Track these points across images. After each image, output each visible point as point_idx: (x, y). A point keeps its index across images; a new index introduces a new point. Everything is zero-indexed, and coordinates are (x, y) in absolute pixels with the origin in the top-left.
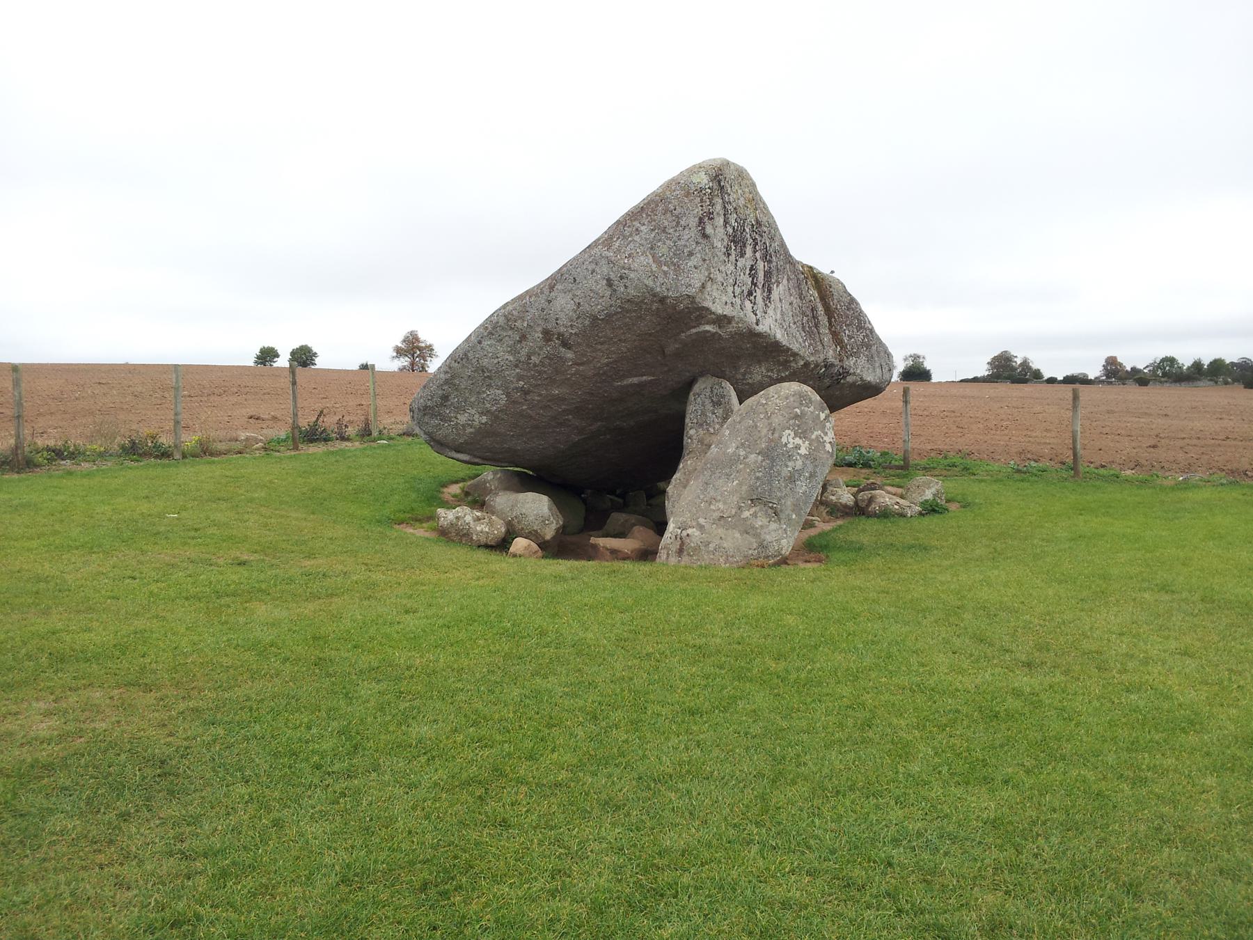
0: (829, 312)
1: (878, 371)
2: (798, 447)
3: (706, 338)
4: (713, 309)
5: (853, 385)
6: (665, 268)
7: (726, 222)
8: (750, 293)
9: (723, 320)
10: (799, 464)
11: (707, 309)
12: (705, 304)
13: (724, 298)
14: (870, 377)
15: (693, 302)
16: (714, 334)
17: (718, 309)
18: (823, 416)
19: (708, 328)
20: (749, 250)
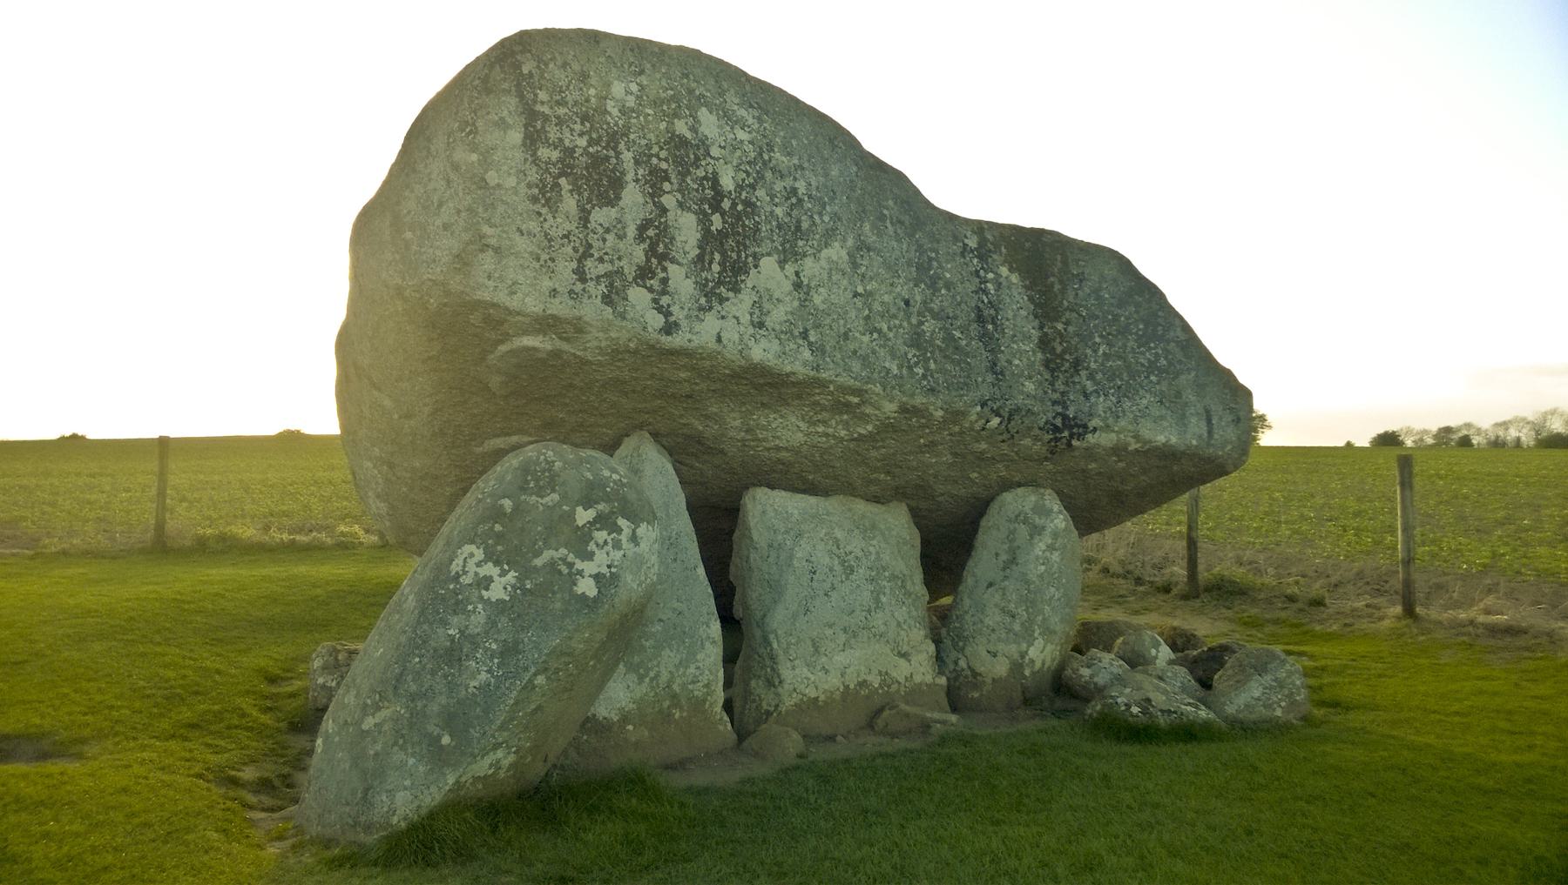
0: (1046, 310)
1: (1196, 427)
2: (486, 582)
3: (530, 363)
4: (514, 303)
5: (1118, 450)
6: (409, 235)
7: (532, 139)
8: (644, 274)
9: (546, 324)
10: (478, 620)
11: (494, 305)
12: (486, 296)
13: (547, 284)
14: (1164, 435)
15: (448, 293)
16: (556, 354)
17: (533, 305)
18: (583, 516)
19: (529, 341)
20: (632, 196)
